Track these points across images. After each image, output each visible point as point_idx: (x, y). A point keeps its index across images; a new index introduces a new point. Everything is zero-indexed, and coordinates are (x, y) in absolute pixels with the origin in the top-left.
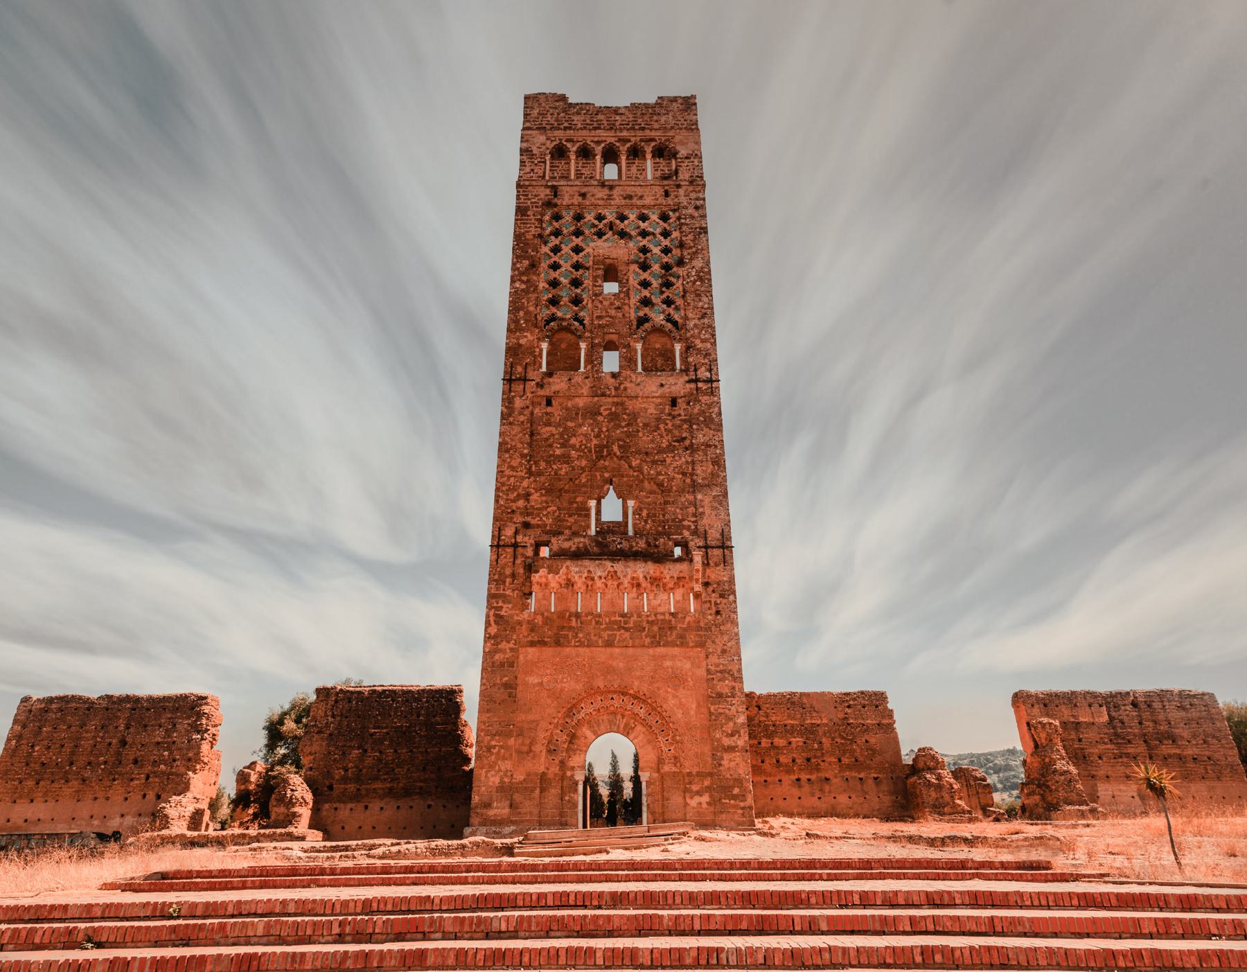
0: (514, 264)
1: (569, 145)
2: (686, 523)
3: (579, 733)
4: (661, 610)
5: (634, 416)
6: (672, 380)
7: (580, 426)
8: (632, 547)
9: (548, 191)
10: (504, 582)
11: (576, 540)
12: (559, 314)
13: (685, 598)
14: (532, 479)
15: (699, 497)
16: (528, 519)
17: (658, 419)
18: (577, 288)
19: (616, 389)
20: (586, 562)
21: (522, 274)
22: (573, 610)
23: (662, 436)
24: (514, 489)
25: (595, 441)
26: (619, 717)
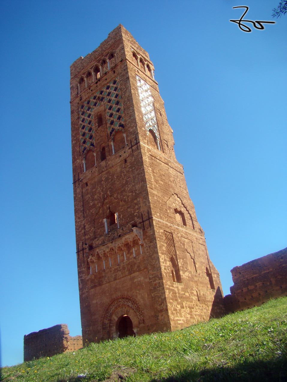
0: (72, 135)
3: (112, 319)
7: (97, 189)
10: (82, 266)
12: (86, 146)
13: (139, 249)
18: (90, 132)
19: (106, 167)
21: (74, 137)
24: (81, 225)
25: (102, 193)
26: (124, 308)
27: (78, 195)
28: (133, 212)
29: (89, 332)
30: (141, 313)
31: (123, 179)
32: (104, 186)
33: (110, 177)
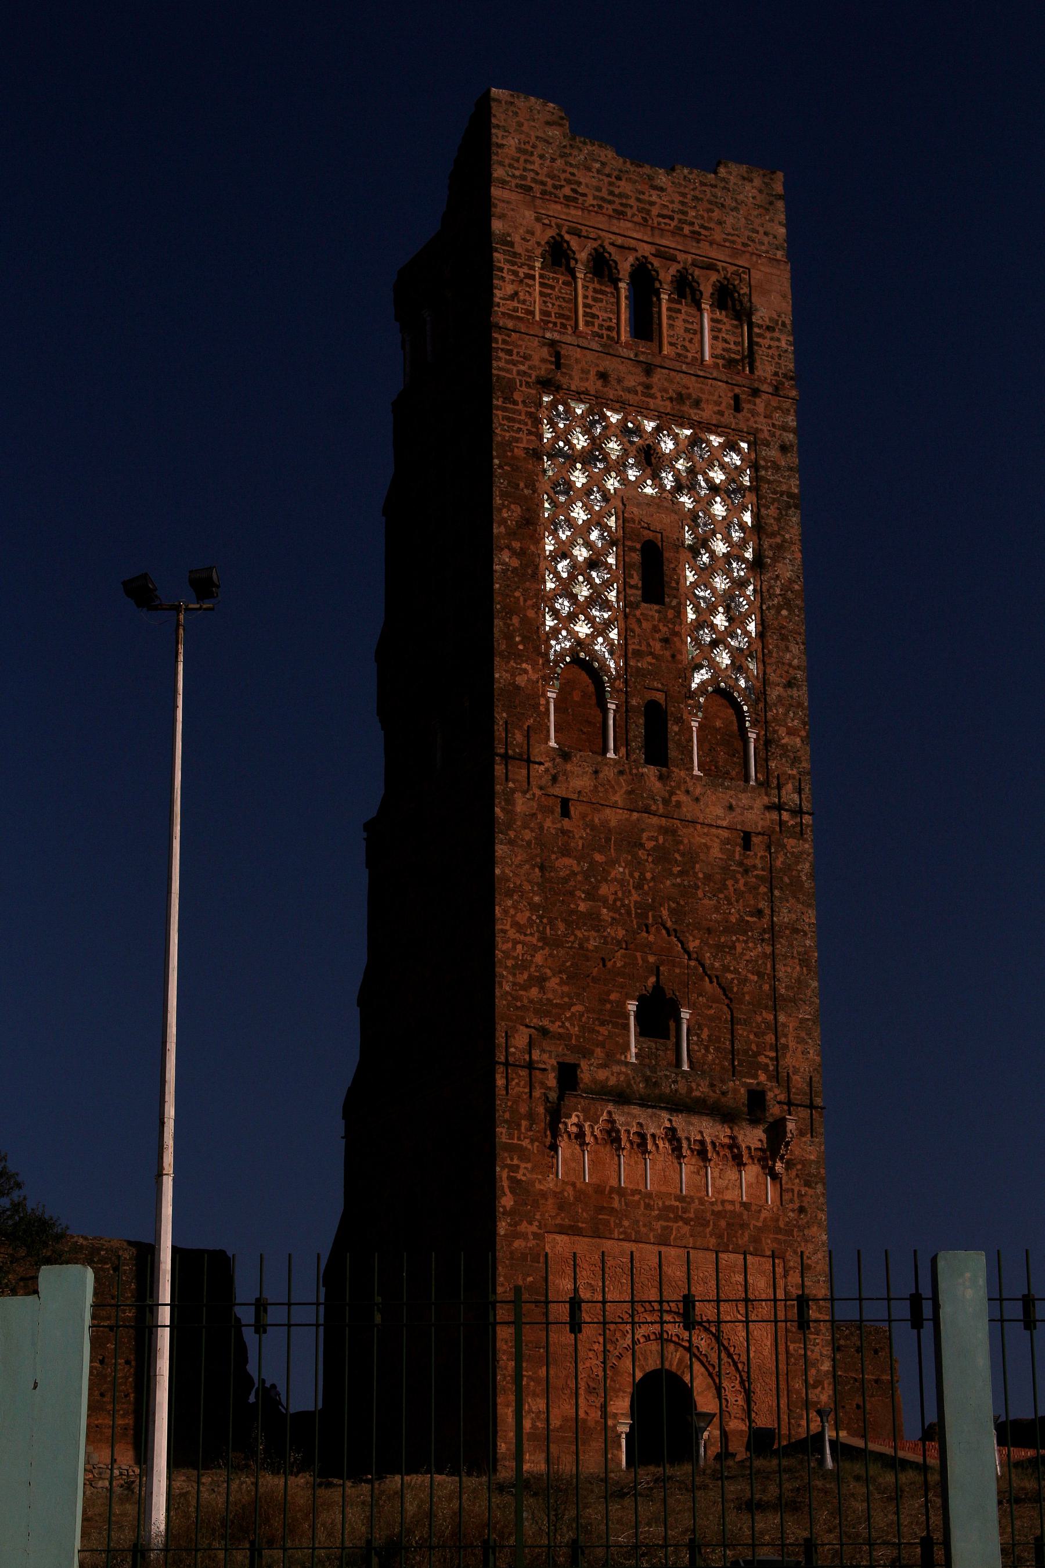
1: (574, 243)
2: (762, 1059)
4: (729, 1196)
5: (691, 857)
6: (745, 799)
7: (612, 863)
8: (690, 1090)
9: (545, 352)
10: (519, 1125)
11: (616, 1069)
14: (547, 951)
15: (782, 1018)
16: (545, 1022)
17: (726, 869)
19: (666, 802)
20: (636, 1110)
22: (614, 1183)
23: (730, 903)
25: (635, 897)
27: (519, 823)
28: (754, 1047)
29: (532, 1384)
30: (738, 1387)
31: (730, 903)
32: (648, 875)
33: (677, 855)
